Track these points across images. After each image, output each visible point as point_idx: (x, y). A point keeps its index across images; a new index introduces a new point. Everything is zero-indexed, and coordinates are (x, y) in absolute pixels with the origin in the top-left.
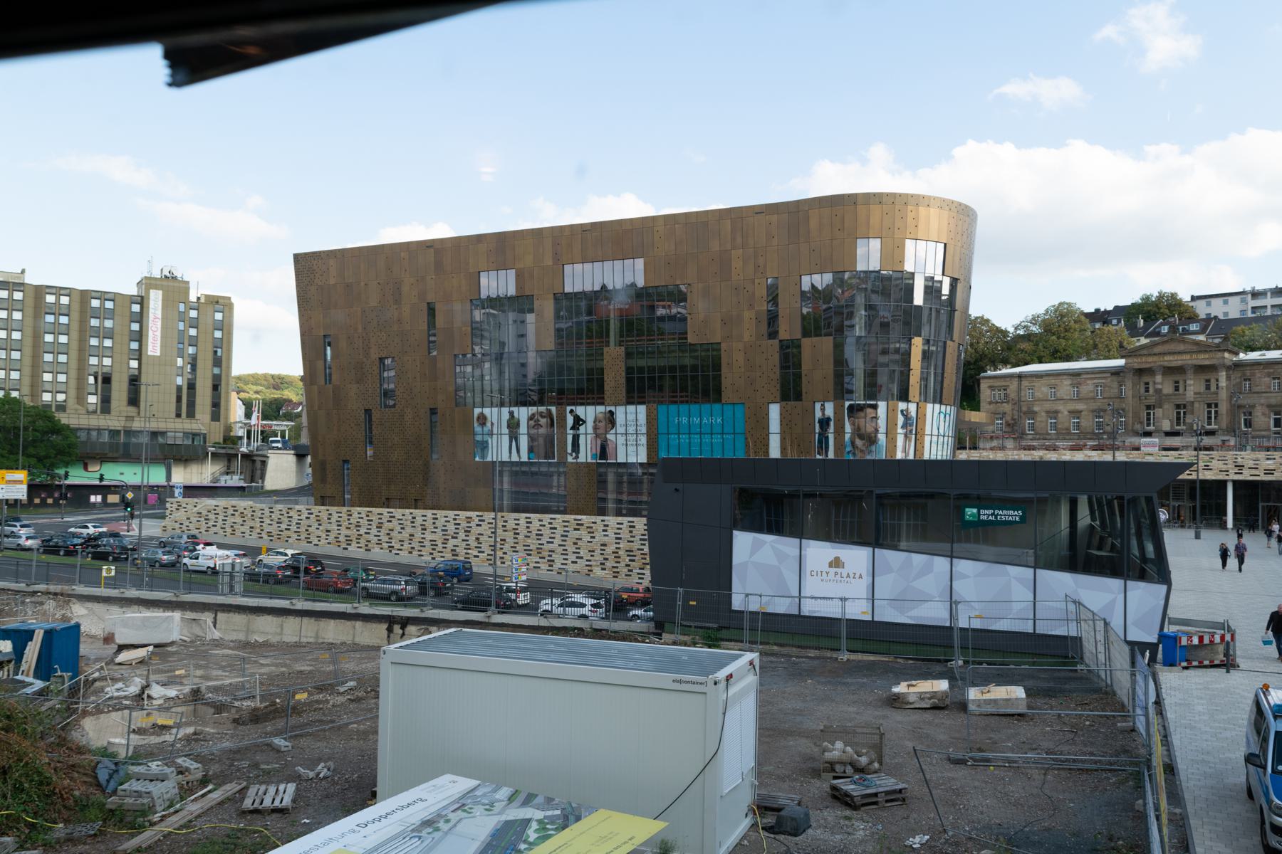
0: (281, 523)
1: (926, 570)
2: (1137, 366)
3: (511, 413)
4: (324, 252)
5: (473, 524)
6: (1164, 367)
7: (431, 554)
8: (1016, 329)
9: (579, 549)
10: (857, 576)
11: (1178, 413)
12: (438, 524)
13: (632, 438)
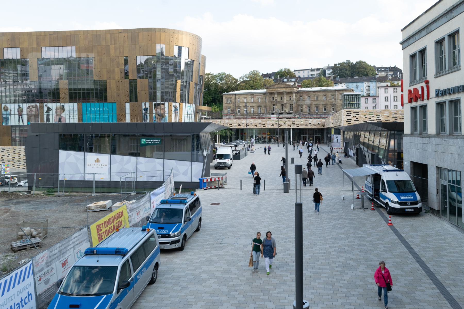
1: (128, 162)
2: (270, 92)
6: (278, 92)
8: (240, 78)
9: (3, 159)
10: (105, 165)
11: (282, 107)
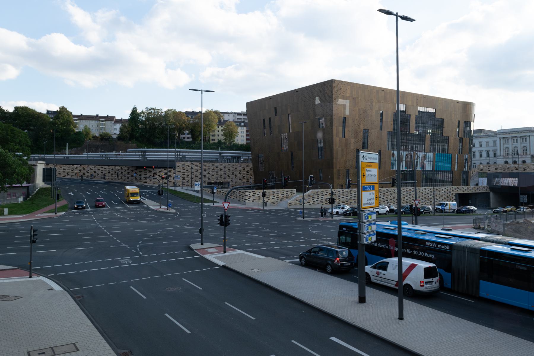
0: (347, 197)
4: (346, 82)
5: (411, 191)
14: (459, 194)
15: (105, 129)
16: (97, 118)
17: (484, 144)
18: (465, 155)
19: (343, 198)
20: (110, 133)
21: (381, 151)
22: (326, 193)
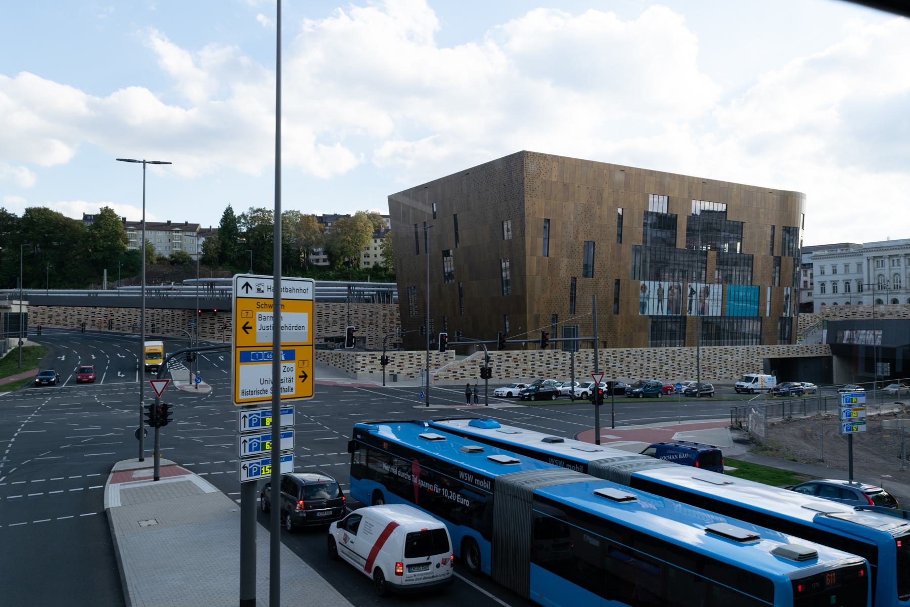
0: (549, 364)
3: (660, 285)
5: (676, 355)
7: (654, 376)
12: (657, 356)
13: (715, 302)
14: (771, 360)
15: (181, 245)
16: (168, 227)
17: (840, 269)
18: (785, 288)
19: (541, 366)
20: (189, 253)
21: (619, 280)
22: (507, 357)
